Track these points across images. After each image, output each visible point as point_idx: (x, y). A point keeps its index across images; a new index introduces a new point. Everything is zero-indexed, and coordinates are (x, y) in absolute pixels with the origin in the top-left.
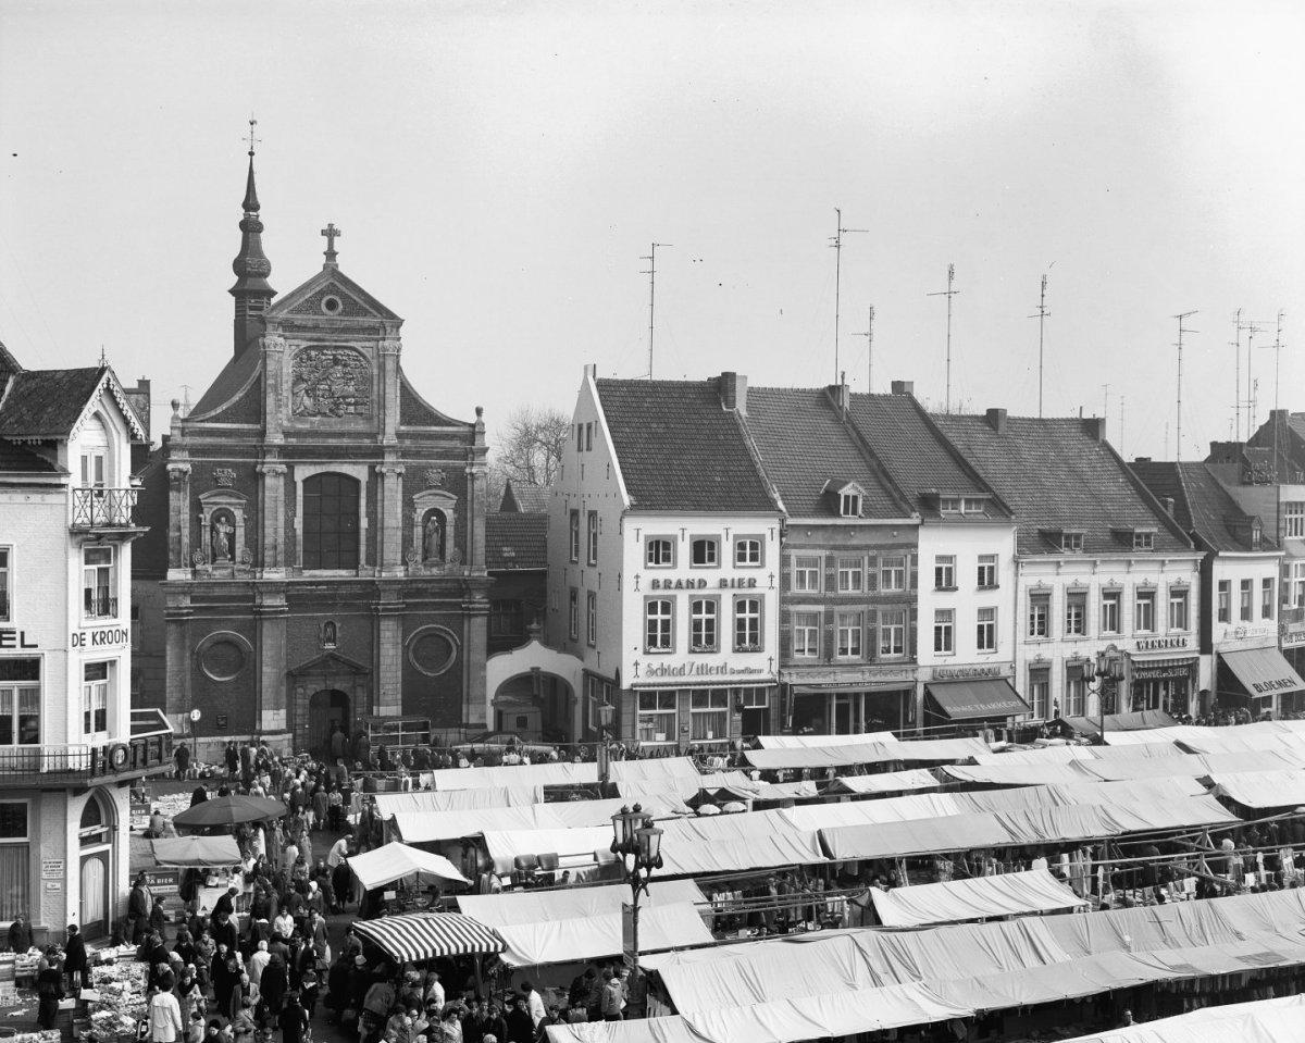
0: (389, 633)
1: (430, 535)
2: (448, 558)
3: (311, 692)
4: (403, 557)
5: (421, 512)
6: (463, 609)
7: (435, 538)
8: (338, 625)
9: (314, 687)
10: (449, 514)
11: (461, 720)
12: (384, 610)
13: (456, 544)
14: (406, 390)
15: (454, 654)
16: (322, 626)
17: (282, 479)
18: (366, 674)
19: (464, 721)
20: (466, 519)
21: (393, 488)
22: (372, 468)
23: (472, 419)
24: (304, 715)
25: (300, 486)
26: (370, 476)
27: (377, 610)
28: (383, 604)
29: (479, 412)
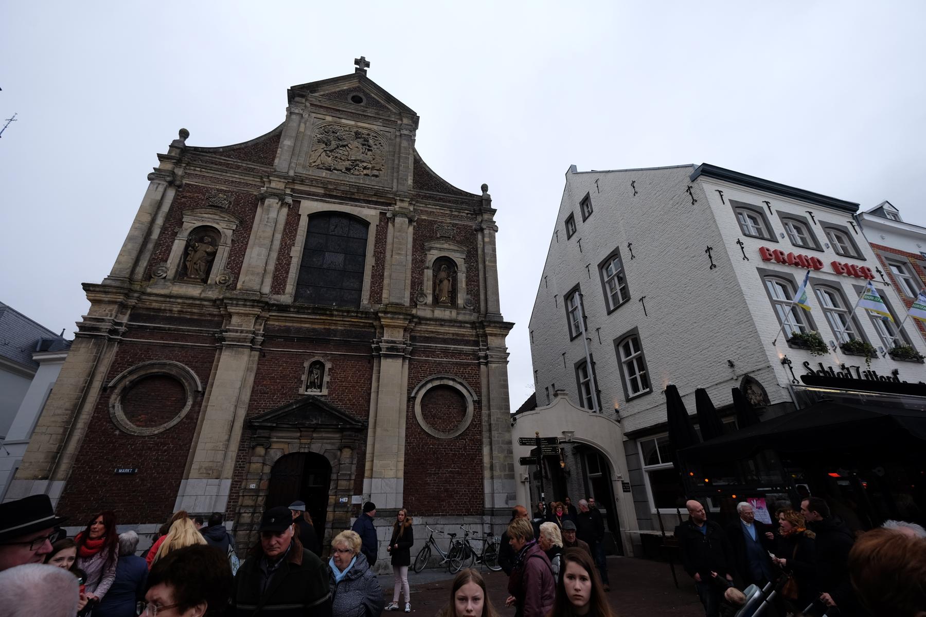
0: (392, 375)
1: (441, 281)
2: (460, 301)
3: (276, 454)
4: (411, 299)
5: (433, 256)
6: (479, 358)
7: (446, 285)
8: (328, 365)
9: (284, 445)
10: (458, 258)
11: (483, 503)
12: (388, 349)
13: (469, 292)
14: (418, 161)
15: (471, 408)
16: (306, 365)
17: (285, 210)
18: (354, 429)
19: (488, 505)
20: (477, 270)
21: (402, 235)
22: (383, 214)
23: (480, 193)
24: (257, 491)
25: (304, 222)
26: (381, 220)
27: (379, 349)
28: (387, 342)
29: (484, 188)
